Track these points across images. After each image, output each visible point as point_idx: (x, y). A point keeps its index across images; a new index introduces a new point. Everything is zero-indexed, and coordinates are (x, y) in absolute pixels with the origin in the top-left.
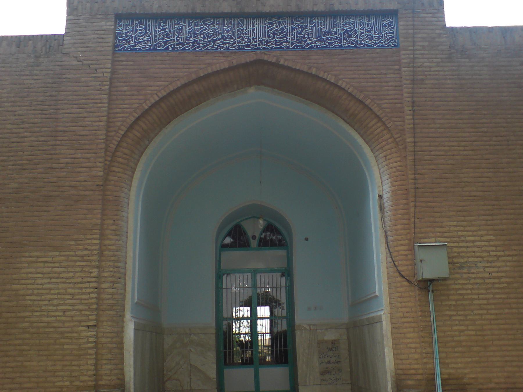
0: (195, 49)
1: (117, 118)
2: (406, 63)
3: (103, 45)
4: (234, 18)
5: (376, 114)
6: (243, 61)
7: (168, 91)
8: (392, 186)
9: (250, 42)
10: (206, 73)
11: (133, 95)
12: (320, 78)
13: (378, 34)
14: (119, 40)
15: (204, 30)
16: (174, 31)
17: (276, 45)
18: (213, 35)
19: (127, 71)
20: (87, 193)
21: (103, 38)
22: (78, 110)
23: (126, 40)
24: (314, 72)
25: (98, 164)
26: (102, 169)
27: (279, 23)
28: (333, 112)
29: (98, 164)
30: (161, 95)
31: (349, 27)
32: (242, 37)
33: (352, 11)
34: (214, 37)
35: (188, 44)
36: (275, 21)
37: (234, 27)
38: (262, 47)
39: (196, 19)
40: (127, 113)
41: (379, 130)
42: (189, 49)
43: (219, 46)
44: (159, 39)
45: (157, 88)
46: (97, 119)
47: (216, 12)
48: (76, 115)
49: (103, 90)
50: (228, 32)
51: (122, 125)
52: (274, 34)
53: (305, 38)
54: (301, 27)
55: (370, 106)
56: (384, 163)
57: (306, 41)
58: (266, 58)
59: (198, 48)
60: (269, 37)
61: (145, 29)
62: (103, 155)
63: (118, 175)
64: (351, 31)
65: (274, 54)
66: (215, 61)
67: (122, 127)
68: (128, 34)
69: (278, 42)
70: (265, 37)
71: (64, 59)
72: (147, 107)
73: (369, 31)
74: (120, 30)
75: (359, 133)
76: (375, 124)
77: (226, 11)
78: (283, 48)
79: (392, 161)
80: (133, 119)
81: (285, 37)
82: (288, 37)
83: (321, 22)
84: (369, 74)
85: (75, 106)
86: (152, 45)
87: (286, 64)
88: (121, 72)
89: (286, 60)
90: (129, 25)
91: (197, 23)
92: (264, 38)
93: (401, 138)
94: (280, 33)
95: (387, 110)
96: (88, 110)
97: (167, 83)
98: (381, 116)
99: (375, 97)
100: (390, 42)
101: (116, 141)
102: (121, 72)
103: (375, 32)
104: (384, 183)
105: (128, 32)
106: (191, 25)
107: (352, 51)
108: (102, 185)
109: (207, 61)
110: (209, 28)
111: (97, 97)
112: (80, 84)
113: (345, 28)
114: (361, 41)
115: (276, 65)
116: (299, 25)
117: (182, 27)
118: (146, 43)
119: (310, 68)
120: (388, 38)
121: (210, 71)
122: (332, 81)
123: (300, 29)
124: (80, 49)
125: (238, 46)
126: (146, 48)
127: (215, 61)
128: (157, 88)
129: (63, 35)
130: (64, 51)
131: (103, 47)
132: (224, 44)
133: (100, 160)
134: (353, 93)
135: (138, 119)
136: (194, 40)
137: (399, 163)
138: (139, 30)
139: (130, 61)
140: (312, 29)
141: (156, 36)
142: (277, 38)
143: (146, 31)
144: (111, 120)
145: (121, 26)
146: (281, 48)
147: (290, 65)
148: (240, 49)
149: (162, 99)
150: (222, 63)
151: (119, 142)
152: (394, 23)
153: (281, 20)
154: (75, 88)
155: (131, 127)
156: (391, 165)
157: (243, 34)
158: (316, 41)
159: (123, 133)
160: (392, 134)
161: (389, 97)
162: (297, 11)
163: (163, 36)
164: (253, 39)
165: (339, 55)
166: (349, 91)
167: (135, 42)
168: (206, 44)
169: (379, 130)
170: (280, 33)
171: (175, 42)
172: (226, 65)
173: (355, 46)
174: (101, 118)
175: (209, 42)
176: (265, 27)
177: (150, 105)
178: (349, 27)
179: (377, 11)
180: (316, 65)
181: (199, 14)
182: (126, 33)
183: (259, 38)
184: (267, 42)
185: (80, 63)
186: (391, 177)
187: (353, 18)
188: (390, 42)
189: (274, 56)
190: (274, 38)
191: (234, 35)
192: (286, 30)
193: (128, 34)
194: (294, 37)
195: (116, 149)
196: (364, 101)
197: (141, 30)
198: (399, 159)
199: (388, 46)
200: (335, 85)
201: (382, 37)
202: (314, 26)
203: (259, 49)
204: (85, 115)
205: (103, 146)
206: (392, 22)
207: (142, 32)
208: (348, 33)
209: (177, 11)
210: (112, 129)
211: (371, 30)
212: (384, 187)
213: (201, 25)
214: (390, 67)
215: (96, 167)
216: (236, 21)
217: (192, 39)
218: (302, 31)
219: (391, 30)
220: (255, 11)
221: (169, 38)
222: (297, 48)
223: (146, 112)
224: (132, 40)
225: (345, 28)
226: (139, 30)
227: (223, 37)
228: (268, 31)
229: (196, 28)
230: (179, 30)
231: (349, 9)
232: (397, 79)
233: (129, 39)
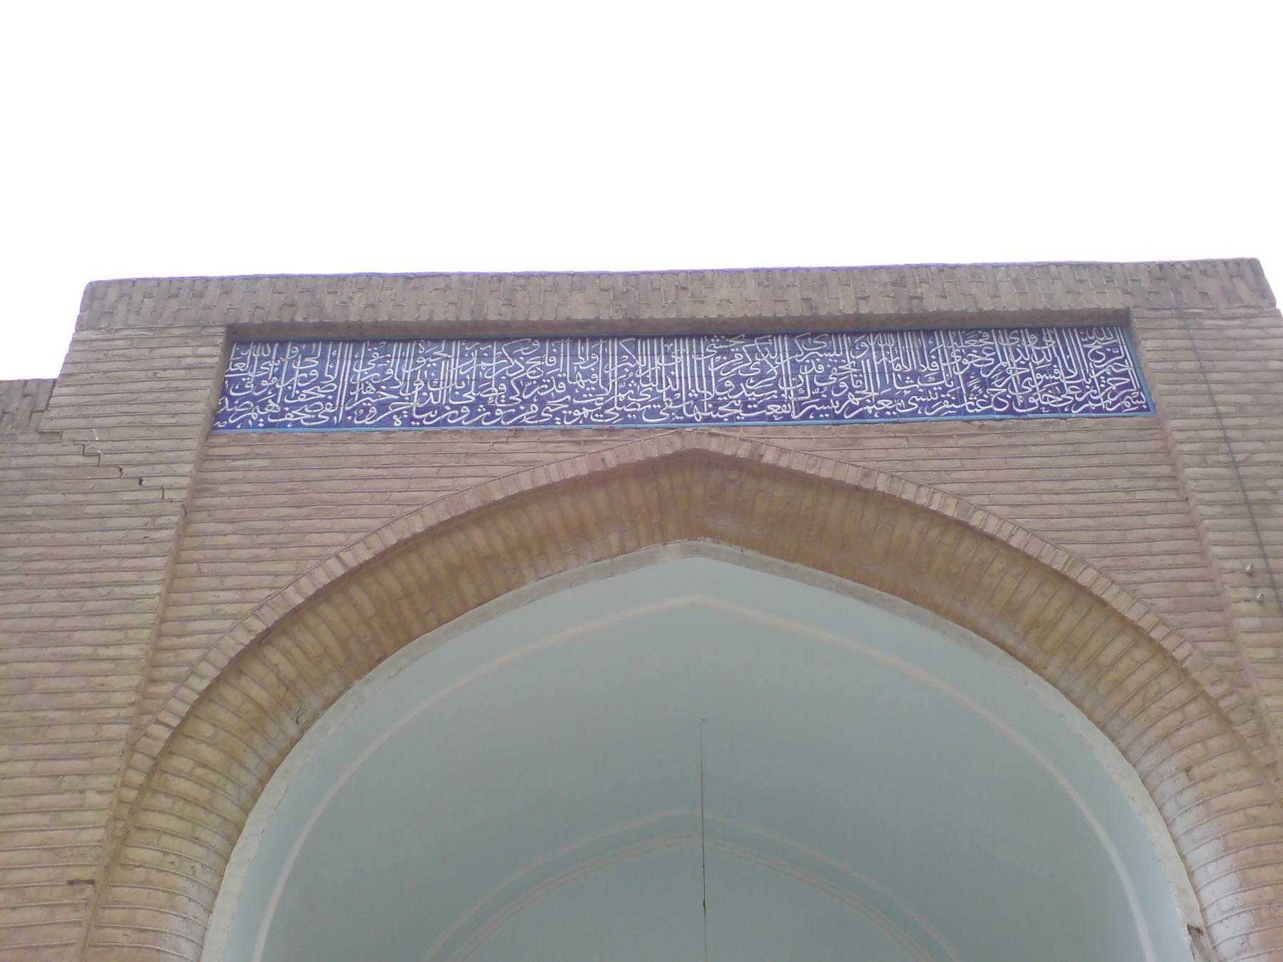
0: (478, 423)
1: (190, 634)
2: (1191, 453)
3: (177, 407)
4: (606, 338)
5: (1123, 619)
6: (639, 456)
7: (379, 548)
8: (1246, 885)
9: (660, 402)
10: (513, 490)
11: (257, 560)
12: (906, 504)
13: (1078, 377)
14: (232, 399)
15: (511, 371)
16: (415, 373)
17: (746, 410)
18: (540, 382)
19: (247, 488)
20: (24, 916)
21: (177, 390)
22: (55, 607)
23: (254, 399)
24: (881, 488)
25: (92, 798)
26: (103, 817)
27: (753, 352)
28: (962, 622)
29: (92, 798)
30: (351, 560)
31: (980, 358)
32: (633, 388)
33: (981, 314)
34: (544, 390)
35: (458, 407)
36: (739, 346)
37: (605, 362)
38: (698, 415)
39: (484, 340)
40: (226, 617)
41: (1141, 675)
42: (459, 424)
43: (555, 414)
44: (361, 396)
45: (341, 538)
46: (116, 636)
47: (549, 317)
48: (45, 623)
49: (154, 542)
50: (587, 375)
51: (204, 658)
52: (737, 380)
53: (838, 390)
55: (1096, 591)
56: (1187, 797)
57: (845, 398)
58: (714, 445)
59: (488, 419)
60: (722, 388)
62: (117, 763)
63: (168, 842)
64: (987, 370)
65: (741, 433)
66: (541, 456)
67: (204, 667)
68: (264, 383)
69: (752, 403)
70: (710, 389)
71: (42, 448)
72: (299, 600)
74: (238, 372)
75: (1067, 694)
76: (1125, 653)
77: (580, 316)
78: (771, 419)
79: (1218, 783)
80: (247, 639)
81: (775, 387)
82: (785, 388)
83: (886, 349)
84: (1068, 492)
85: (46, 593)
86: (337, 414)
87: (784, 462)
88: (223, 488)
89: (782, 451)
90: (269, 358)
91: (489, 351)
92: (705, 392)
93: (1235, 698)
94: (759, 378)
95: (1163, 603)
96: (91, 605)
97: (374, 524)
98: (1143, 624)
99: (1108, 561)
100: (1123, 397)
101: (176, 714)
102: (223, 488)
103: (1067, 373)
104: (1200, 876)
105: (265, 377)
106: (470, 357)
107: (1000, 424)
108: (91, 882)
109: (519, 457)
110: (527, 367)
111: (129, 563)
112: (79, 523)
113: (966, 362)
114: (1026, 397)
115: (752, 468)
116: (813, 357)
117: (439, 363)
118: (319, 407)
119: (867, 474)
120: (1114, 387)
121: (525, 482)
122: (950, 512)
123: (821, 367)
124: (98, 421)
125: (623, 414)
126: (317, 419)
127: (541, 456)
128: (341, 538)
129: (55, 381)
130: (46, 425)
131: (174, 415)
132: (573, 407)
133: (101, 782)
134: (1030, 550)
135: (264, 638)
136: (478, 398)
137: (1249, 794)
138: (301, 372)
139: (258, 456)
140: (858, 366)
141: (352, 387)
142: (749, 391)
143: (321, 371)
144: (165, 642)
145: (244, 360)
146: (761, 418)
147: (798, 464)
148: (627, 421)
149: (354, 575)
150: (568, 463)
151: (185, 720)
152: (1124, 349)
153: (756, 344)
154: (58, 535)
155: (237, 666)
156: (1216, 803)
157: (637, 380)
158: (877, 398)
159: (202, 685)
160: (1195, 683)
161: (1156, 561)
162: (807, 314)
163: (378, 387)
164: (670, 394)
165: (960, 436)
166: (1014, 542)
167: (283, 404)
168: (517, 407)
169: (1141, 675)
170: (759, 378)
171: (416, 404)
172: (583, 468)
173: (1010, 411)
174: (131, 633)
175: (530, 401)
176: (708, 362)
177: (311, 591)
178: (980, 358)
179: (1062, 313)
180: (886, 464)
181: (495, 325)
182: (257, 381)
183: (688, 391)
185: (94, 460)
186: (1227, 849)
187: (986, 335)
188: (1123, 397)
189: (743, 440)
190: (738, 390)
191: (605, 380)
192: (774, 369)
193: (264, 383)
194: (804, 387)
195: (170, 741)
196: (1073, 574)
197: (307, 371)
198: (1244, 776)
199: (1119, 410)
200: (963, 527)
201: (1093, 383)
202: (865, 359)
203: (692, 420)
204: (78, 622)
205: (124, 729)
206: (1116, 346)
207: (310, 378)
208: (978, 375)
209: (424, 318)
210: (165, 672)
211: (1051, 367)
212: (1206, 895)
213: (503, 357)
214: (1140, 469)
215: (82, 808)
216: (614, 346)
217: (471, 396)
218: (828, 371)
219: (1116, 367)
220: (673, 315)
221: (396, 392)
222: (817, 418)
223: (296, 614)
224: (274, 400)
225: (966, 362)
226: (301, 372)
228: (717, 373)
229: (483, 364)
230: (430, 371)
231: (972, 310)
232: (1170, 506)
233: (265, 395)
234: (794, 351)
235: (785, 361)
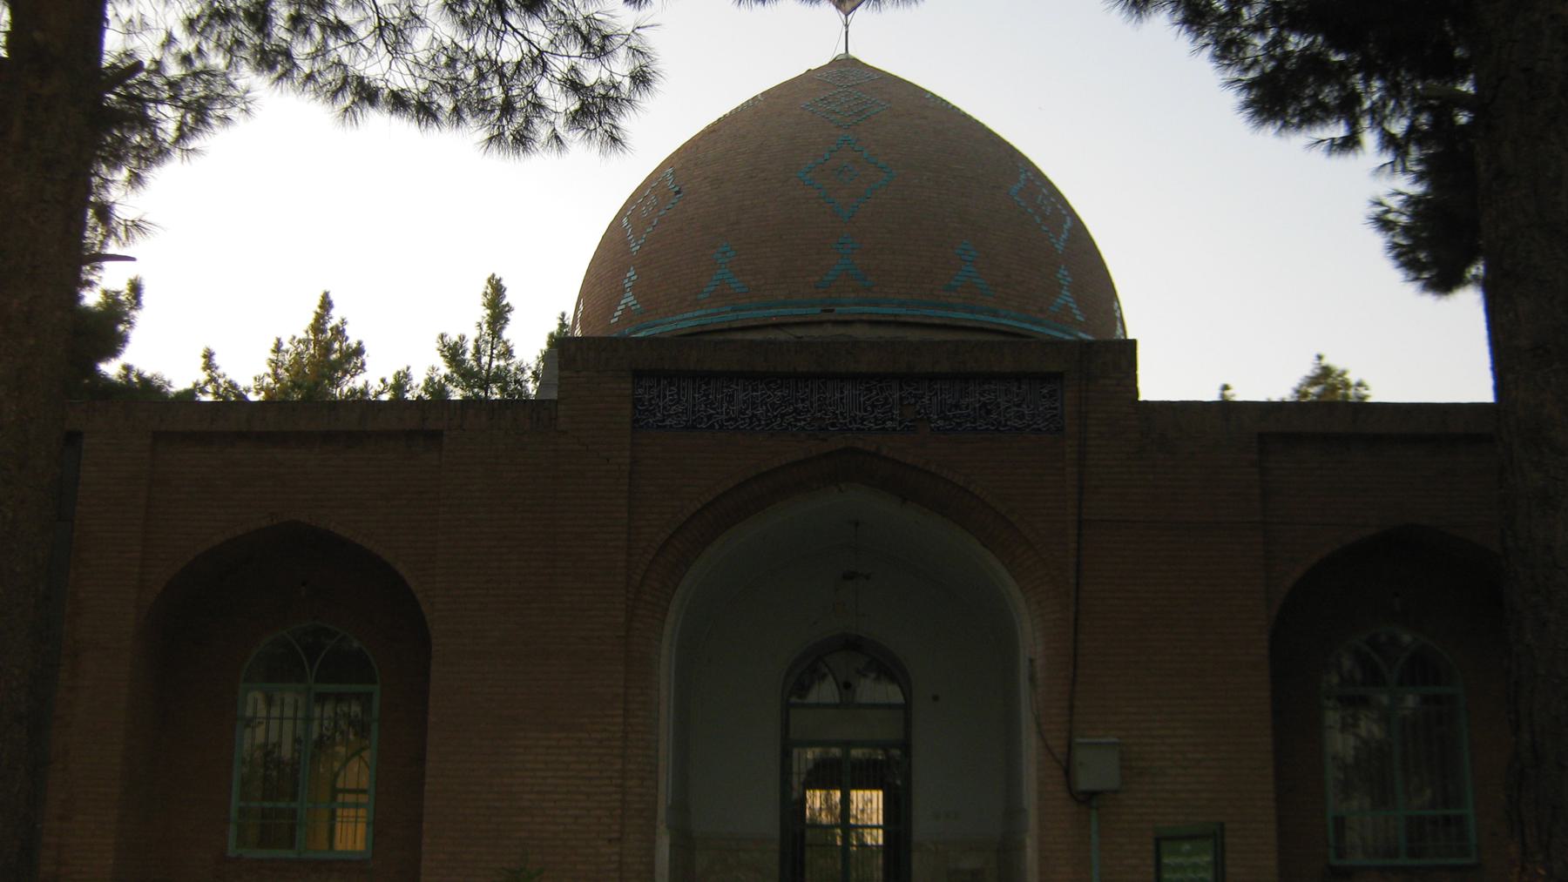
38: (855, 426)
52: (873, 406)
73: (1019, 406)
184: (863, 419)
234: (901, 389)
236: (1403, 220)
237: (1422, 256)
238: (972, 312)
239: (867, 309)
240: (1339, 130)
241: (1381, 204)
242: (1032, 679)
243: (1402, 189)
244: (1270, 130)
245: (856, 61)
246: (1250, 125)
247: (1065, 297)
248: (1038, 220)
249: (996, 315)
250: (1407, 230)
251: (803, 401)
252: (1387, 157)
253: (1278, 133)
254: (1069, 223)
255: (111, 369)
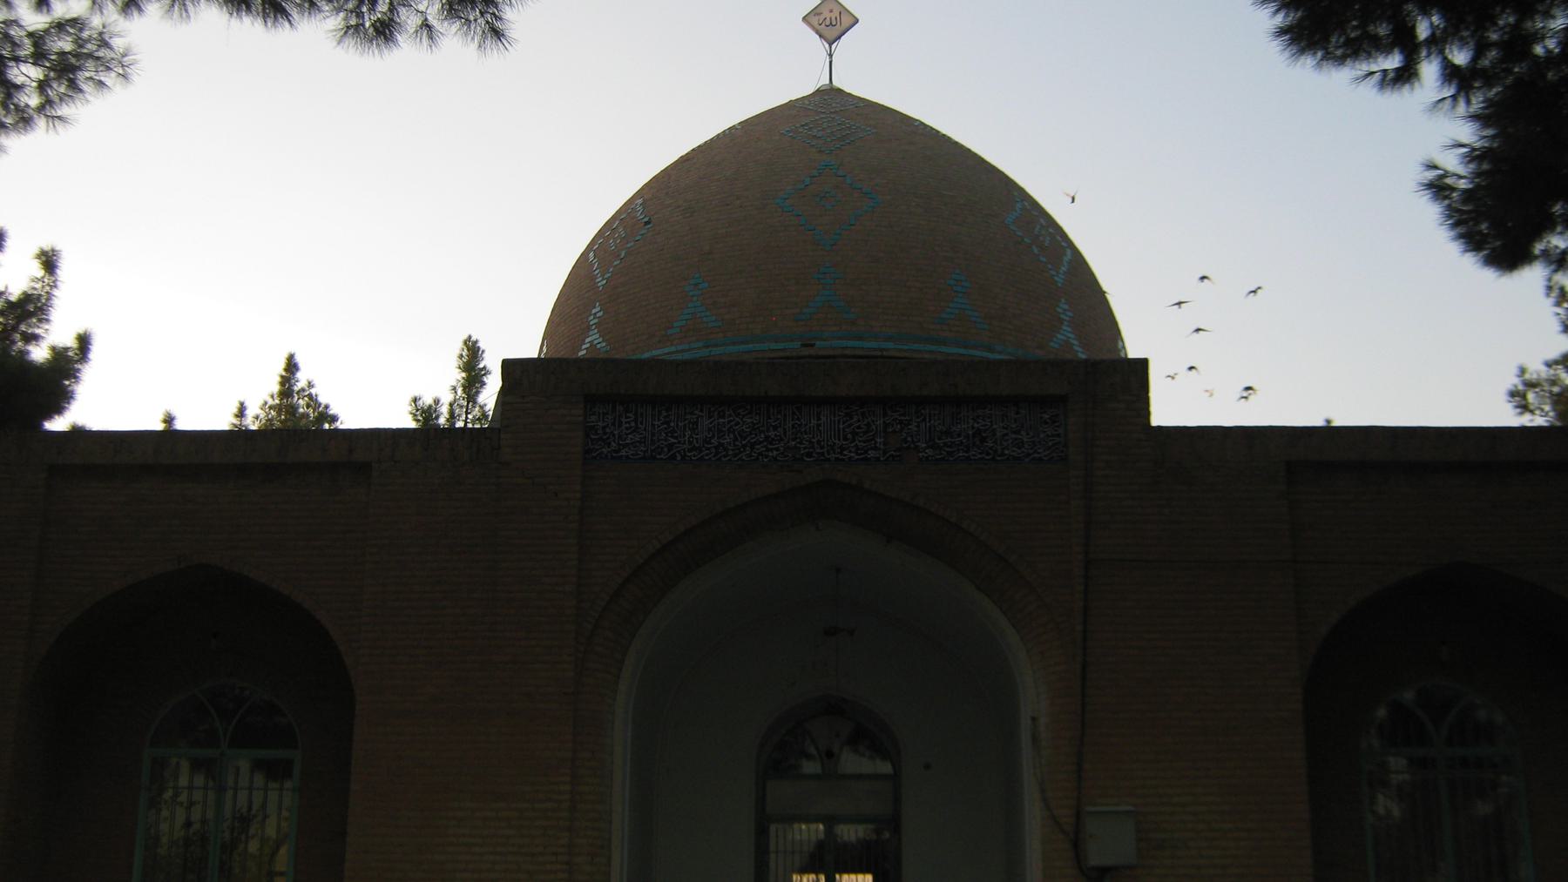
27: (863, 414)
54: (901, 422)
61: (636, 421)
173: (993, 459)
175: (744, 446)
184: (842, 449)
227: (767, 438)
234: (885, 415)
235: (880, 422)
236: (1463, 184)
237: (1484, 227)
238: (965, 347)
239: (851, 343)
240: (1393, 62)
241: (1436, 167)
242: (1035, 739)
243: (1465, 140)
244: (1308, 61)
245: (840, 91)
246: (1287, 54)
247: (1066, 333)
248: (1036, 250)
249: (990, 350)
250: (1468, 195)
251: (775, 428)
252: (1449, 92)
253: (1319, 65)
254: (1069, 252)
255: (58, 424)
